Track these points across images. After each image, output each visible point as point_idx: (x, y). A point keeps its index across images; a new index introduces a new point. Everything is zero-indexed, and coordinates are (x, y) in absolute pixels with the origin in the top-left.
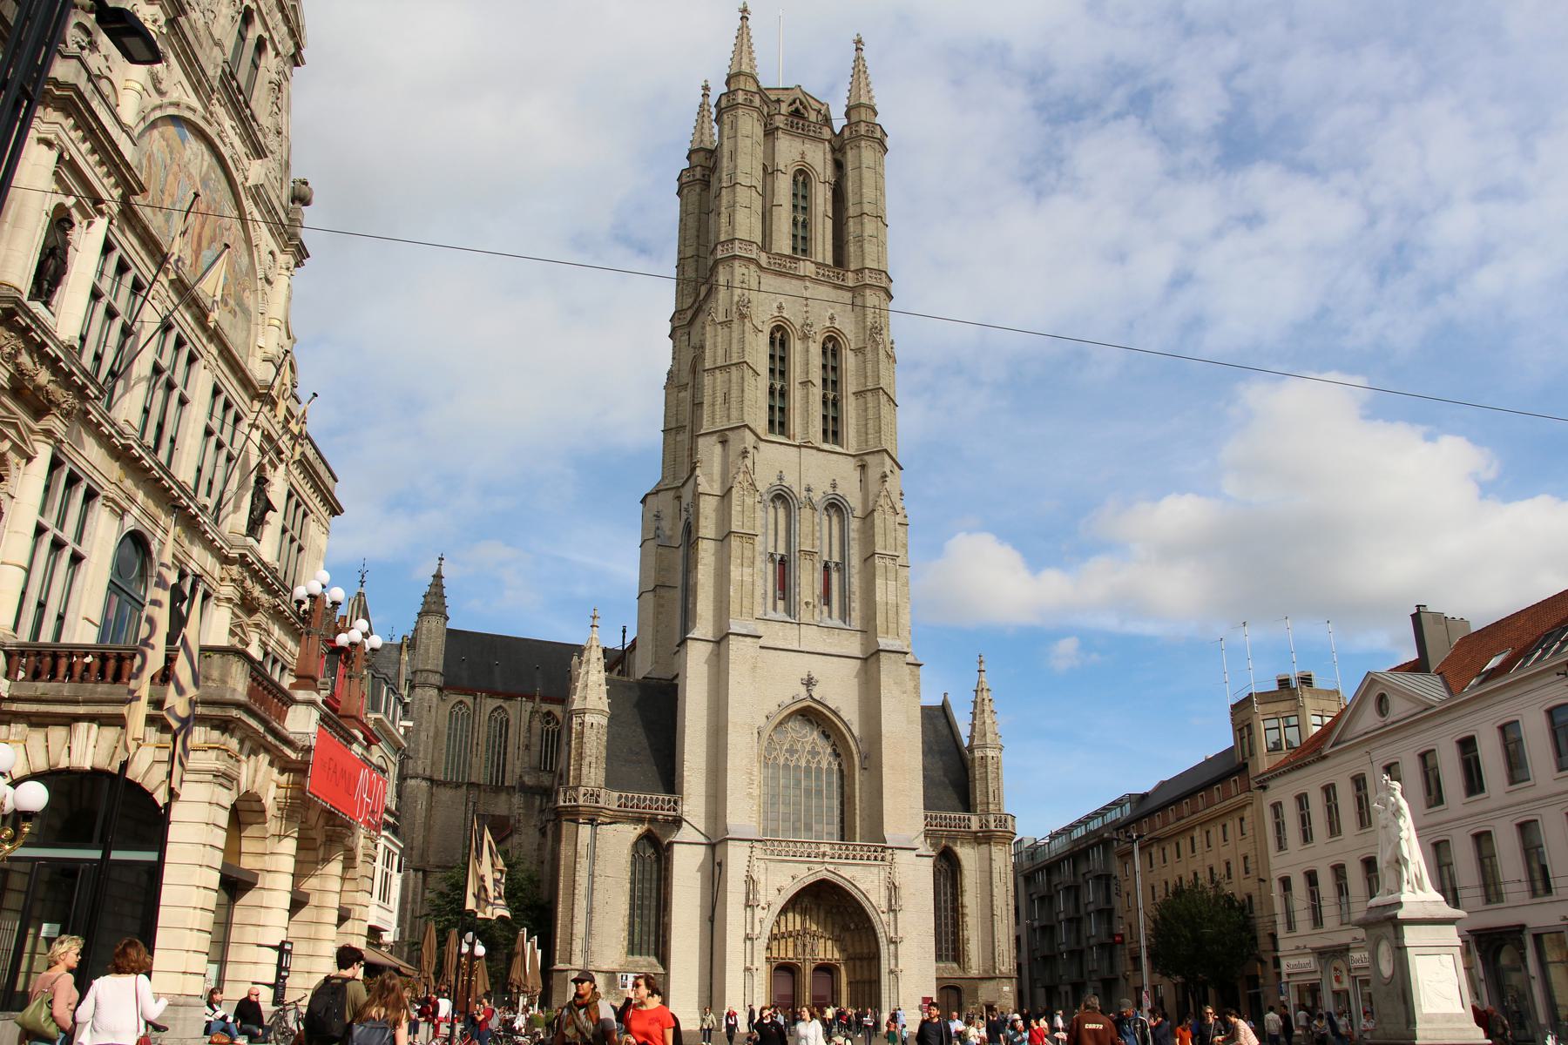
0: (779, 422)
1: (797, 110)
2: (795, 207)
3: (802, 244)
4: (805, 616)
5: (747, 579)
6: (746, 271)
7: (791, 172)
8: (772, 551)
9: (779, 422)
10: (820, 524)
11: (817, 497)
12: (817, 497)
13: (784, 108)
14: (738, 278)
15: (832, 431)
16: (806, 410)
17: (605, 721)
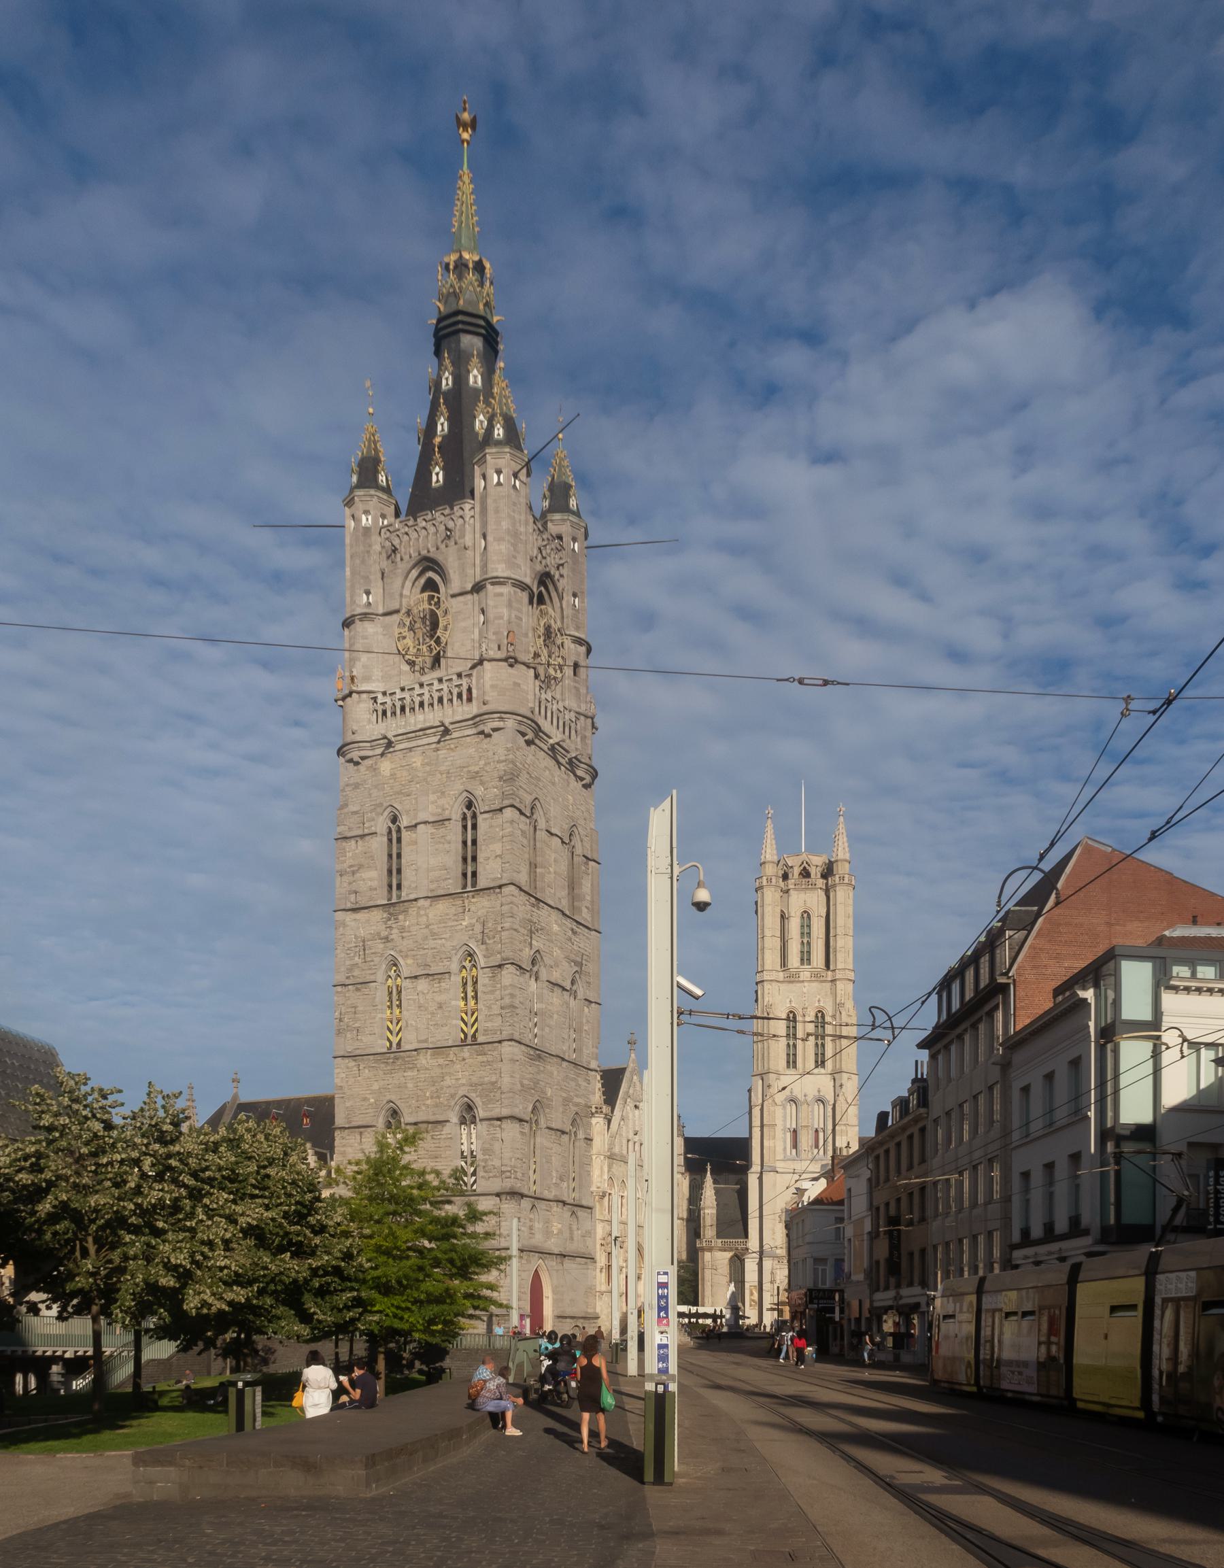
0: (792, 1062)
1: (805, 868)
2: (802, 934)
3: (806, 958)
4: (803, 1155)
5: (772, 1145)
6: (769, 987)
7: (799, 914)
8: (788, 1126)
9: (792, 1062)
10: (813, 1111)
11: (809, 1098)
12: (809, 1098)
13: (797, 871)
14: (766, 991)
15: (820, 1062)
16: (807, 1051)
17: (714, 1211)
